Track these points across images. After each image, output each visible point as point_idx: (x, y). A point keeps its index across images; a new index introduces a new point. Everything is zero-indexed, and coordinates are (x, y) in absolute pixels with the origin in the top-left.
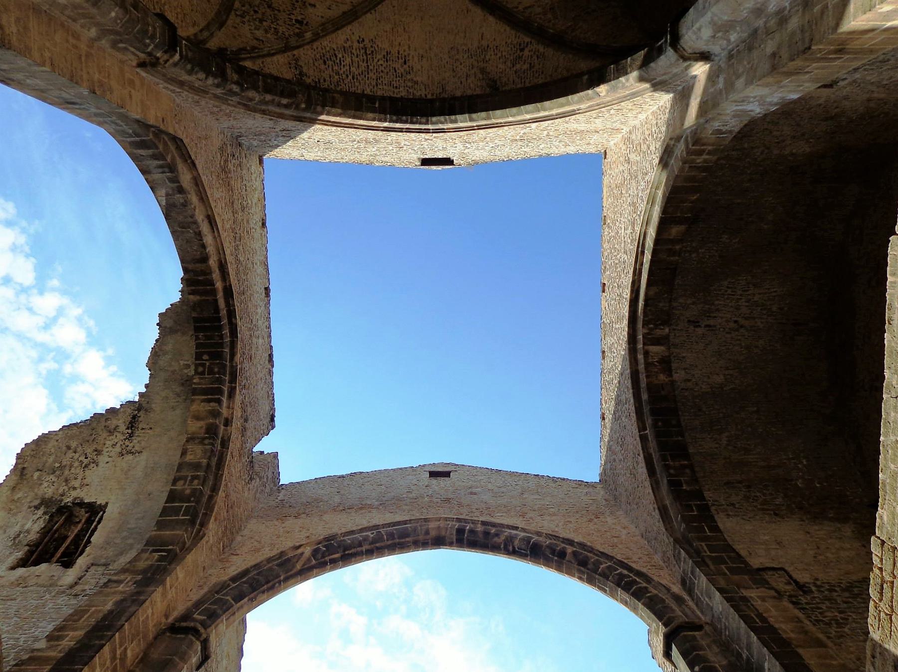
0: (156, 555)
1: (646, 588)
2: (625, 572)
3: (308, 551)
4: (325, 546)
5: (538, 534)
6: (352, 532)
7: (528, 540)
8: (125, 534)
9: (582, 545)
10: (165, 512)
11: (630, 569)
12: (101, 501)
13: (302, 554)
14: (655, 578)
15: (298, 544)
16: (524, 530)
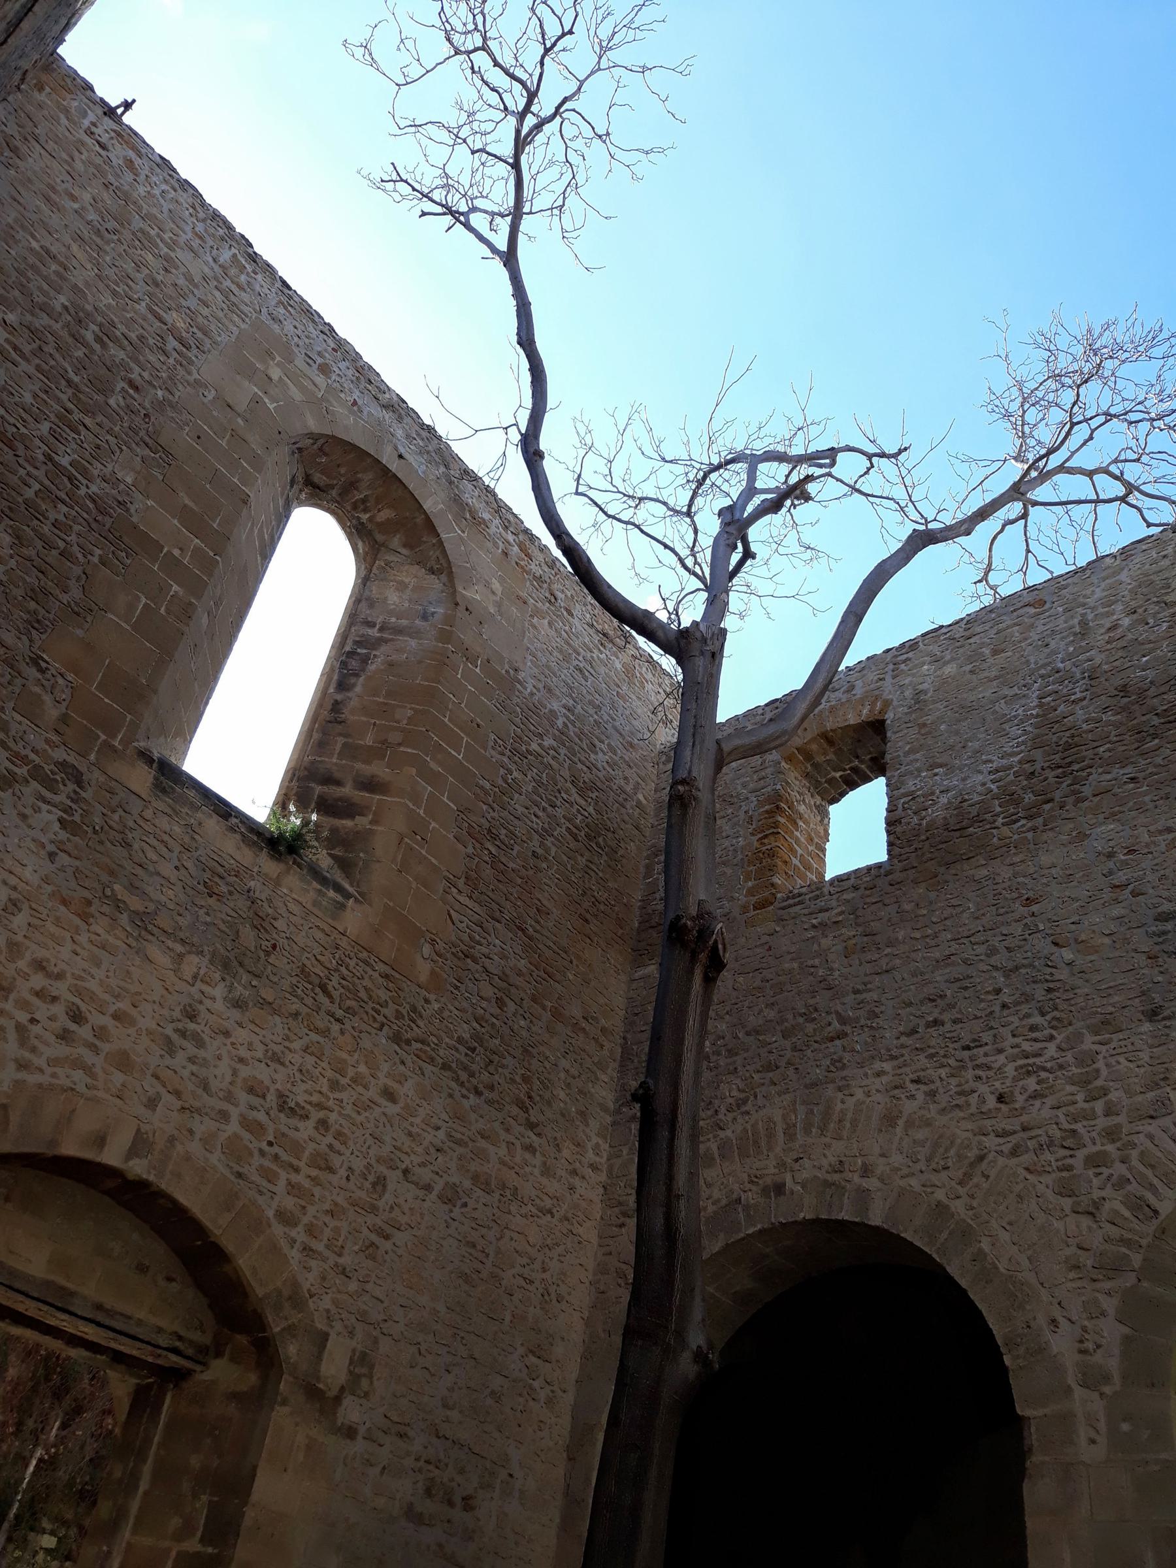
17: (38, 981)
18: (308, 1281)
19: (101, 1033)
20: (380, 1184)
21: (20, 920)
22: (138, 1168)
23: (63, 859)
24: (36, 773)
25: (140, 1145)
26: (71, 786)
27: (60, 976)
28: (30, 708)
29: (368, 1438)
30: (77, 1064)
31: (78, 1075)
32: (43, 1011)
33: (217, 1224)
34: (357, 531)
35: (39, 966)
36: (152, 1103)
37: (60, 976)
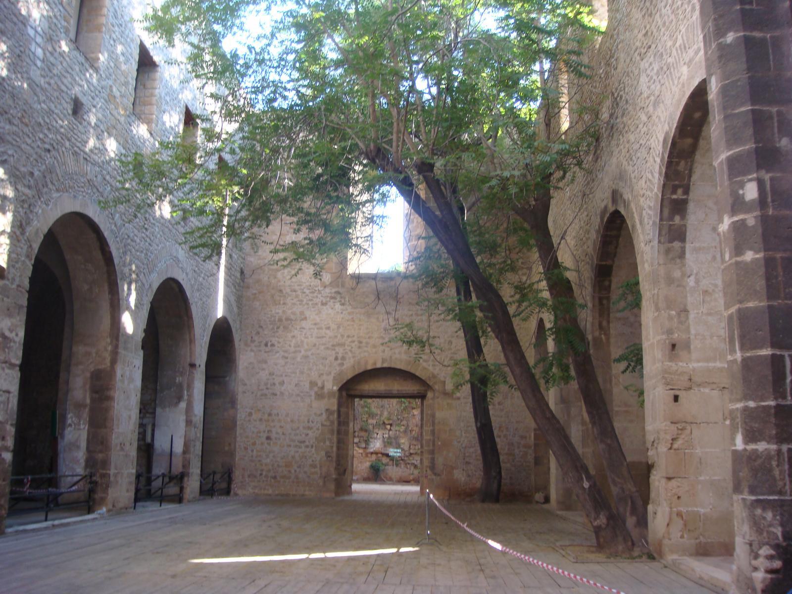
17: (350, 340)
18: (436, 372)
19: (367, 343)
21: (341, 330)
22: (385, 365)
23: (344, 312)
24: (332, 298)
25: (384, 361)
26: (339, 296)
27: (354, 336)
29: (464, 398)
30: (365, 351)
31: (366, 354)
32: (353, 345)
35: (348, 336)
36: (384, 351)
37: (354, 336)
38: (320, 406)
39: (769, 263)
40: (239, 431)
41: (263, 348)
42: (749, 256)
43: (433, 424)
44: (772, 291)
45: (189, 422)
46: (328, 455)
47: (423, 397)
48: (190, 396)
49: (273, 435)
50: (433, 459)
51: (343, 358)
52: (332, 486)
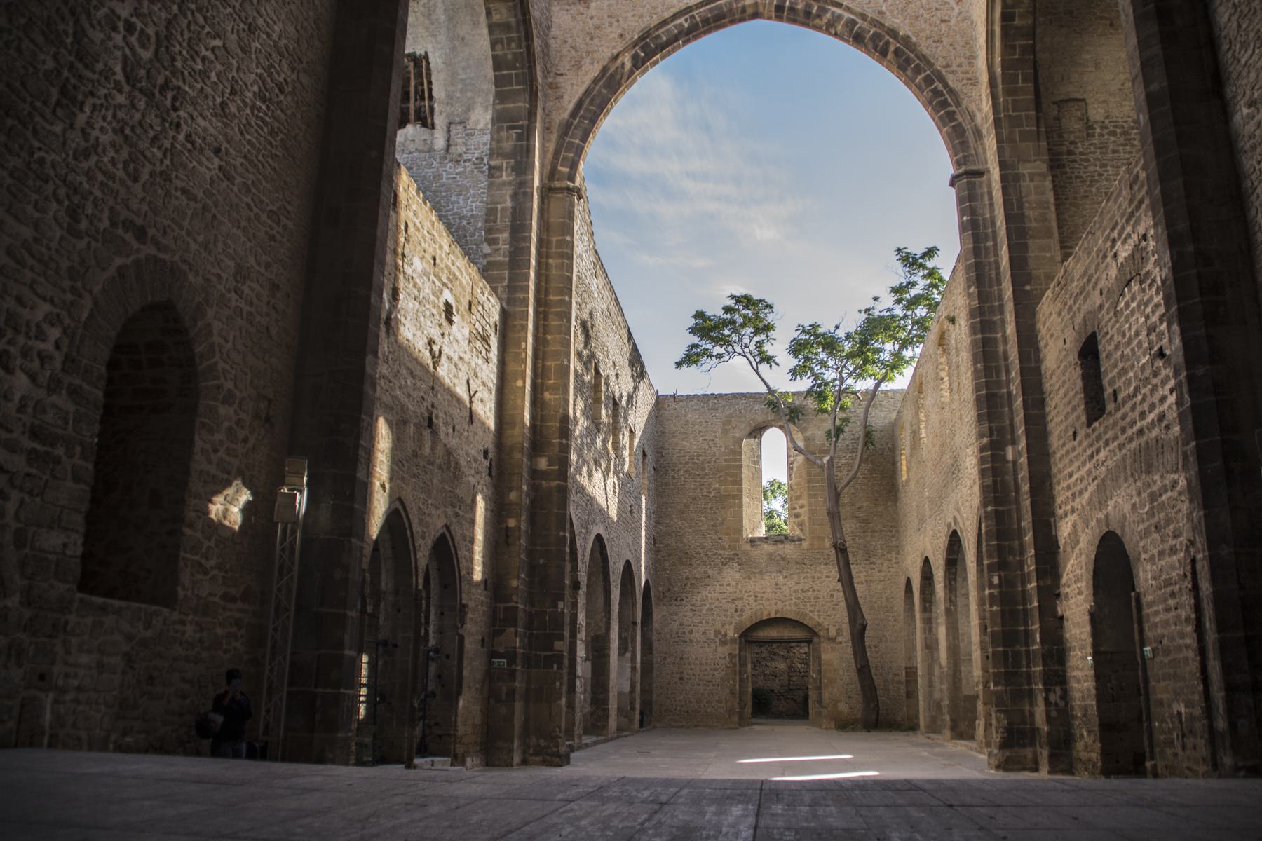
0: (513, 132)
1: (954, 112)
2: (940, 87)
3: (627, 60)
4: (642, 49)
5: (863, 17)
6: (665, 22)
7: (854, 23)
8: (460, 86)
9: (906, 40)
10: (498, 81)
11: (946, 85)
12: (420, 51)
13: (623, 64)
14: (965, 103)
15: (615, 52)
16: (848, 9)
20: (832, 596)
25: (776, 612)
28: (723, 548)
33: (797, 618)
34: (781, 427)
38: (723, 651)
39: (1002, 611)
40: (655, 673)
41: (673, 602)
42: (995, 608)
43: (820, 665)
44: (1003, 624)
45: (633, 669)
46: (732, 692)
47: (809, 642)
48: (634, 647)
49: (685, 676)
50: (820, 695)
51: (742, 610)
52: (736, 719)
